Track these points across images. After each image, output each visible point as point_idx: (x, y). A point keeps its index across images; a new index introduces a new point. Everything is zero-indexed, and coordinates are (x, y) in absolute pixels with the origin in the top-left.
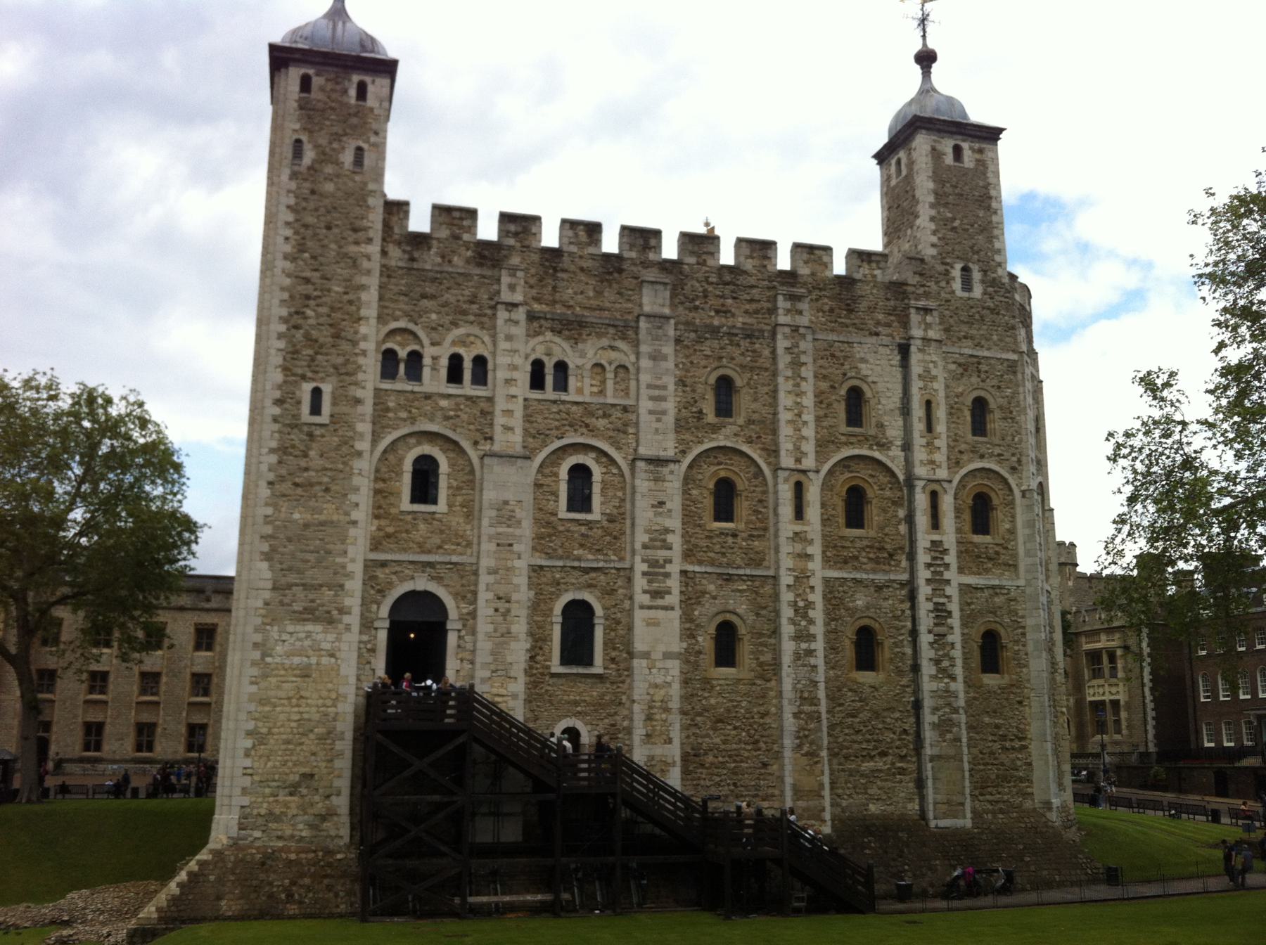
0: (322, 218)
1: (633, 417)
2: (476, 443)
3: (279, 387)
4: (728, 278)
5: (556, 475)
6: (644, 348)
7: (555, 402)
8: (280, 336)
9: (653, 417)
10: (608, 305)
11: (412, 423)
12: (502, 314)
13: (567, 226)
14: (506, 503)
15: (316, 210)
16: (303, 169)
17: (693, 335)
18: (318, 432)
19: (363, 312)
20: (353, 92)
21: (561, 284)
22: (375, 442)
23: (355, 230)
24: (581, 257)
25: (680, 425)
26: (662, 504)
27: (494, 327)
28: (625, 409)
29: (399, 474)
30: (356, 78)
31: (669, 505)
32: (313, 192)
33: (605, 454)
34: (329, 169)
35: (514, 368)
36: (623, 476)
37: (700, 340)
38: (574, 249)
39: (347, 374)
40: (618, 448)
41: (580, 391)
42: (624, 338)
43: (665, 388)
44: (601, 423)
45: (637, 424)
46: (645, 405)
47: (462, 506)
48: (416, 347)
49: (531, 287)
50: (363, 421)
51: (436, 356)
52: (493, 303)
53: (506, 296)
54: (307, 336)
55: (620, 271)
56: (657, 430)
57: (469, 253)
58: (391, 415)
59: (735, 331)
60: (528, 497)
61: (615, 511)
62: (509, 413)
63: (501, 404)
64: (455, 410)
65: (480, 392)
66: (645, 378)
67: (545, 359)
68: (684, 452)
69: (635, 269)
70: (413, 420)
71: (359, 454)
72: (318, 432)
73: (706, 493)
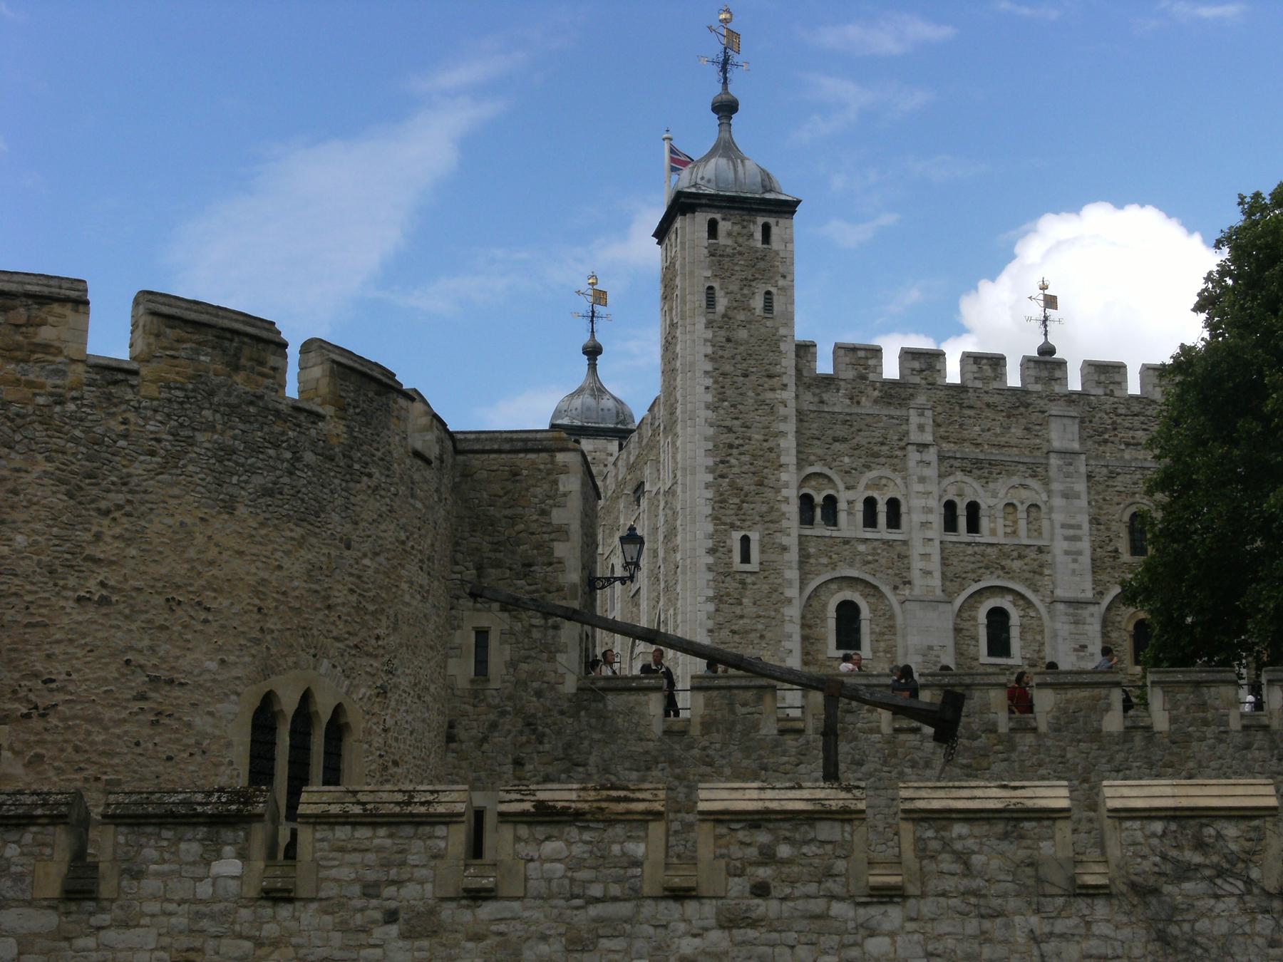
0: (739, 366)
1: (1048, 558)
2: (896, 588)
3: (711, 536)
4: (1136, 409)
5: (975, 619)
6: (1056, 486)
7: (969, 544)
8: (708, 486)
9: (1069, 558)
10: (1013, 441)
11: (833, 569)
12: (913, 456)
13: (971, 361)
14: (930, 648)
15: (733, 358)
16: (717, 317)
17: (1105, 471)
18: (750, 580)
19: (783, 460)
20: (758, 235)
21: (967, 421)
22: (801, 589)
23: (770, 376)
24: (986, 392)
25: (1097, 566)
26: (1083, 647)
27: (905, 469)
28: (1040, 550)
29: (824, 620)
30: (761, 220)
31: (1091, 649)
32: (729, 340)
33: (1023, 597)
34: (741, 316)
35: (928, 510)
36: (1040, 619)
37: (1112, 475)
38: (979, 384)
39: (772, 521)
40: (1036, 591)
41: (993, 532)
42: (1034, 476)
43: (1079, 527)
44: (1016, 565)
45: (1052, 565)
46: (1060, 546)
47: (886, 652)
48: (832, 492)
49: (939, 426)
50: (790, 568)
51: (850, 500)
52: (902, 444)
53: (915, 436)
54: (732, 484)
55: (1027, 406)
56: (1074, 571)
57: (876, 393)
58: (812, 561)
59: (1148, 465)
60: (950, 642)
61: (1035, 656)
62: (925, 556)
63: (917, 549)
64: (873, 554)
65: (894, 535)
66: (1058, 517)
67: (957, 500)
68: (1101, 593)
69: (1042, 403)
70: (834, 566)
71: (790, 601)
72: (750, 580)
73: (1126, 636)
